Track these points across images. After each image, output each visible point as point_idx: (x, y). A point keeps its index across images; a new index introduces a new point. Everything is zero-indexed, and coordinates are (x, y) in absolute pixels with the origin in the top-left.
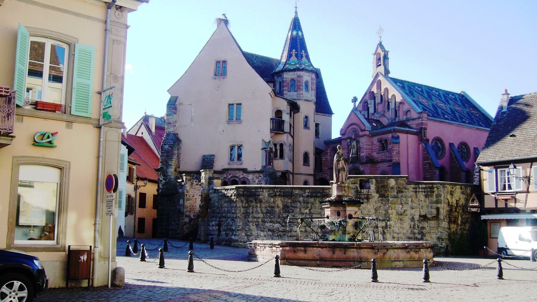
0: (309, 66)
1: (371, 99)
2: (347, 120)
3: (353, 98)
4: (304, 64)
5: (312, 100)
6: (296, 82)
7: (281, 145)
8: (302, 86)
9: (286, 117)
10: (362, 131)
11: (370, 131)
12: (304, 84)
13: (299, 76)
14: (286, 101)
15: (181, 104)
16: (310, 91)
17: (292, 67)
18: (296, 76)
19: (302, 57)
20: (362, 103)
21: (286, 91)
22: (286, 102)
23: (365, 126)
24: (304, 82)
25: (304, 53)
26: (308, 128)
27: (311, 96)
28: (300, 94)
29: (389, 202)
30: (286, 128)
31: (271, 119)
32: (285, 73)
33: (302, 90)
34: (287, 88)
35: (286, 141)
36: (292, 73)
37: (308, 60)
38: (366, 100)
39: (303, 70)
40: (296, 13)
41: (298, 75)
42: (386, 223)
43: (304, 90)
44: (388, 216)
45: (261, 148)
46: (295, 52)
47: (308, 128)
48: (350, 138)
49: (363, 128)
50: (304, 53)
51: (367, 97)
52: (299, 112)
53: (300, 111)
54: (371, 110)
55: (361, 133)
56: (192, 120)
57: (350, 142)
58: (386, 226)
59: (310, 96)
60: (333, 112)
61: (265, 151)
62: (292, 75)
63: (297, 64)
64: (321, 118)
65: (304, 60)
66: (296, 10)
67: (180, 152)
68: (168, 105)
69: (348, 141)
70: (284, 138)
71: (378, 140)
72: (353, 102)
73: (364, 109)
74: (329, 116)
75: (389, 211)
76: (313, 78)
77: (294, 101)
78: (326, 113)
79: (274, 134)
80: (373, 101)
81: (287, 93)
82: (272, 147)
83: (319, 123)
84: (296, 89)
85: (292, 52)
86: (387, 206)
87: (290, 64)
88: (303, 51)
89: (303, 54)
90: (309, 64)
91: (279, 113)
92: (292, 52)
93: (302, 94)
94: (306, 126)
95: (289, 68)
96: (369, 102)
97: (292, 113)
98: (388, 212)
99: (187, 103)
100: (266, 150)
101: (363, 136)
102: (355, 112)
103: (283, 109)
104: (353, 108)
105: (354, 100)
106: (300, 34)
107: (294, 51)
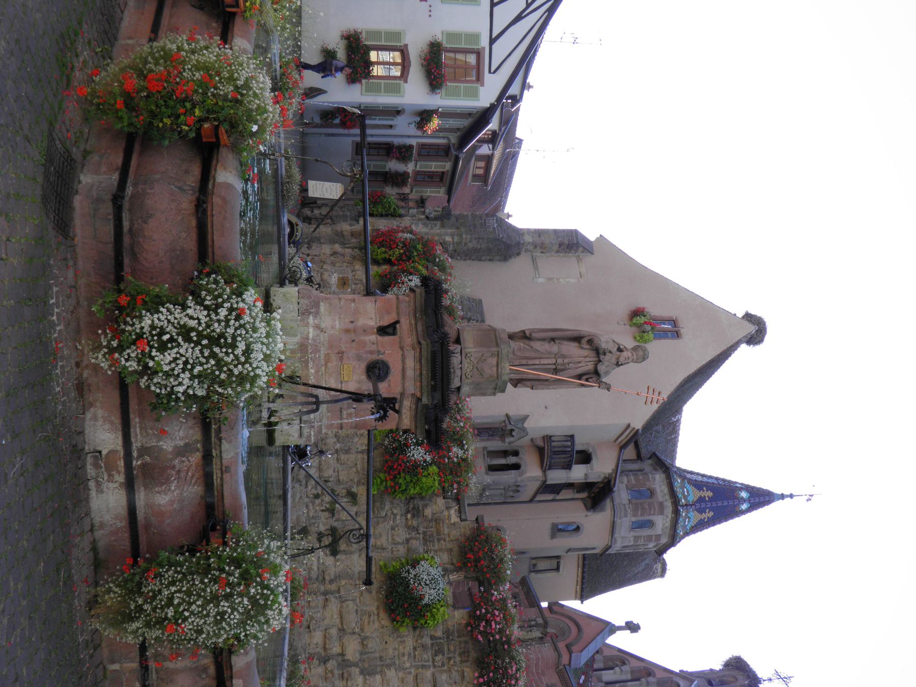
0: (684, 527)
1: (632, 672)
2: (585, 613)
3: (635, 622)
4: (687, 516)
5: (615, 540)
6: (650, 500)
7: (516, 467)
8: (642, 515)
9: (578, 473)
10: (568, 647)
11: (569, 665)
12: (646, 518)
13: (661, 506)
14: (613, 470)
15: (579, 260)
16: (632, 534)
17: (678, 490)
18: (661, 499)
19: (701, 511)
20: (621, 654)
21: (628, 481)
22: (610, 471)
23: (582, 651)
24: (651, 518)
25: (708, 517)
26: (553, 536)
27: (623, 538)
28: (626, 510)
29: (420, 670)
30: (557, 476)
31: (572, 437)
32: (663, 476)
33: (634, 516)
34: (634, 482)
35: (528, 474)
36: (666, 490)
37: (696, 526)
38: (627, 660)
39: (676, 512)
40: (782, 497)
41: (665, 504)
42: (355, 665)
43: (634, 519)
44: (379, 669)
45: (510, 414)
46: (708, 497)
47: (553, 536)
48: (546, 624)
49: (573, 648)
50: (708, 517)
51: (635, 663)
52: (588, 509)
53: (589, 513)
54: (608, 676)
55: (561, 645)
56: (550, 279)
57: (537, 625)
58: (345, 664)
59: (622, 534)
60: (584, 602)
61: (505, 421)
62: (662, 491)
63: (685, 500)
64: (571, 571)
65: (694, 517)
66: (787, 496)
67: (483, 258)
68: (576, 232)
69: (540, 621)
70: (532, 471)
71: (552, 684)
72: (627, 623)
73: (607, 659)
74: (576, 591)
75: (393, 670)
76: (660, 540)
77: (614, 486)
78: (583, 583)
79: (541, 444)
80: (629, 677)
81: (623, 483)
82: (513, 436)
83: (561, 572)
84: (634, 501)
85: (707, 491)
86: (408, 665)
87: (683, 487)
88: (712, 514)
89: (705, 513)
90: (688, 528)
91: (585, 458)
92: (707, 491)
93: (626, 516)
94: (557, 530)
95: (676, 484)
96: (626, 668)
97: (584, 495)
98: (388, 666)
99: (583, 270)
100: (507, 422)
101: (556, 649)
102: (608, 628)
103: (595, 466)
104: (614, 625)
105: (632, 625)
106: (744, 507)
107: (710, 494)
